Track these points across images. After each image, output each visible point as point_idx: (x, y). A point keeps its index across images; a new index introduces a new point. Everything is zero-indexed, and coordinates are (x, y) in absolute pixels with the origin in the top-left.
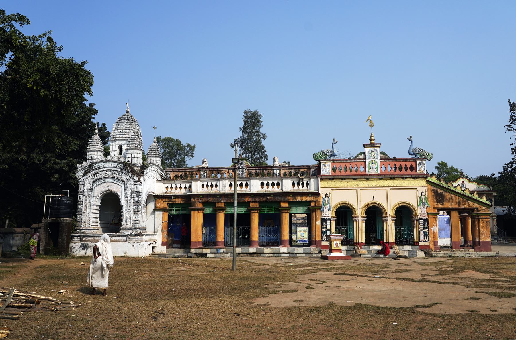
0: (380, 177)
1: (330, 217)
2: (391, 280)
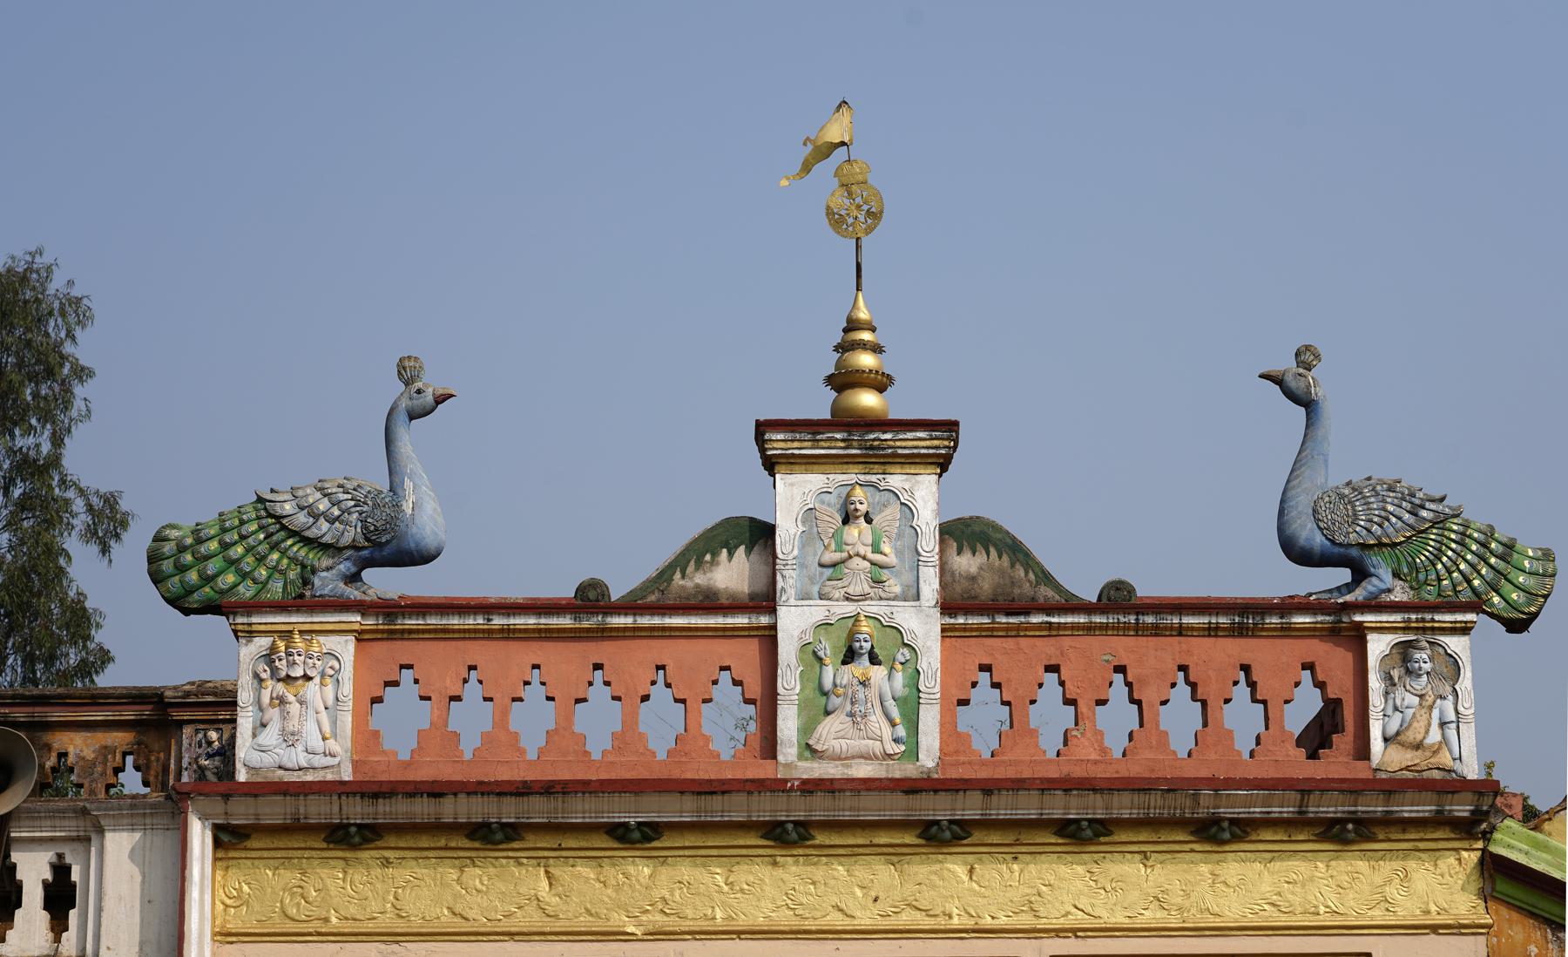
0: (939, 815)
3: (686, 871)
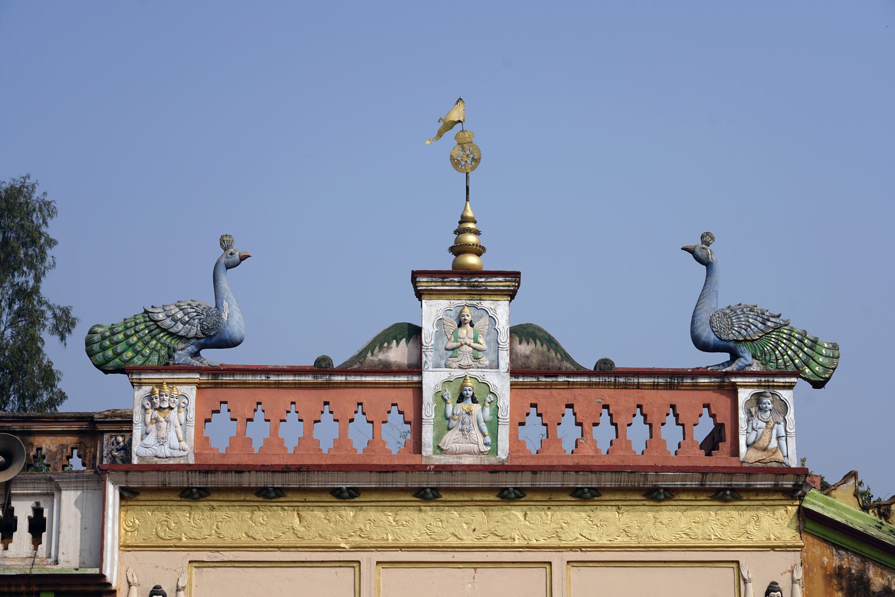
0: (508, 485)
3: (372, 514)
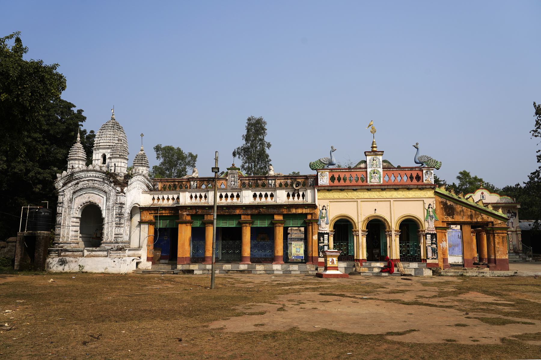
0: (383, 188)
1: (328, 232)
2: (378, 302)
3: (360, 193)
